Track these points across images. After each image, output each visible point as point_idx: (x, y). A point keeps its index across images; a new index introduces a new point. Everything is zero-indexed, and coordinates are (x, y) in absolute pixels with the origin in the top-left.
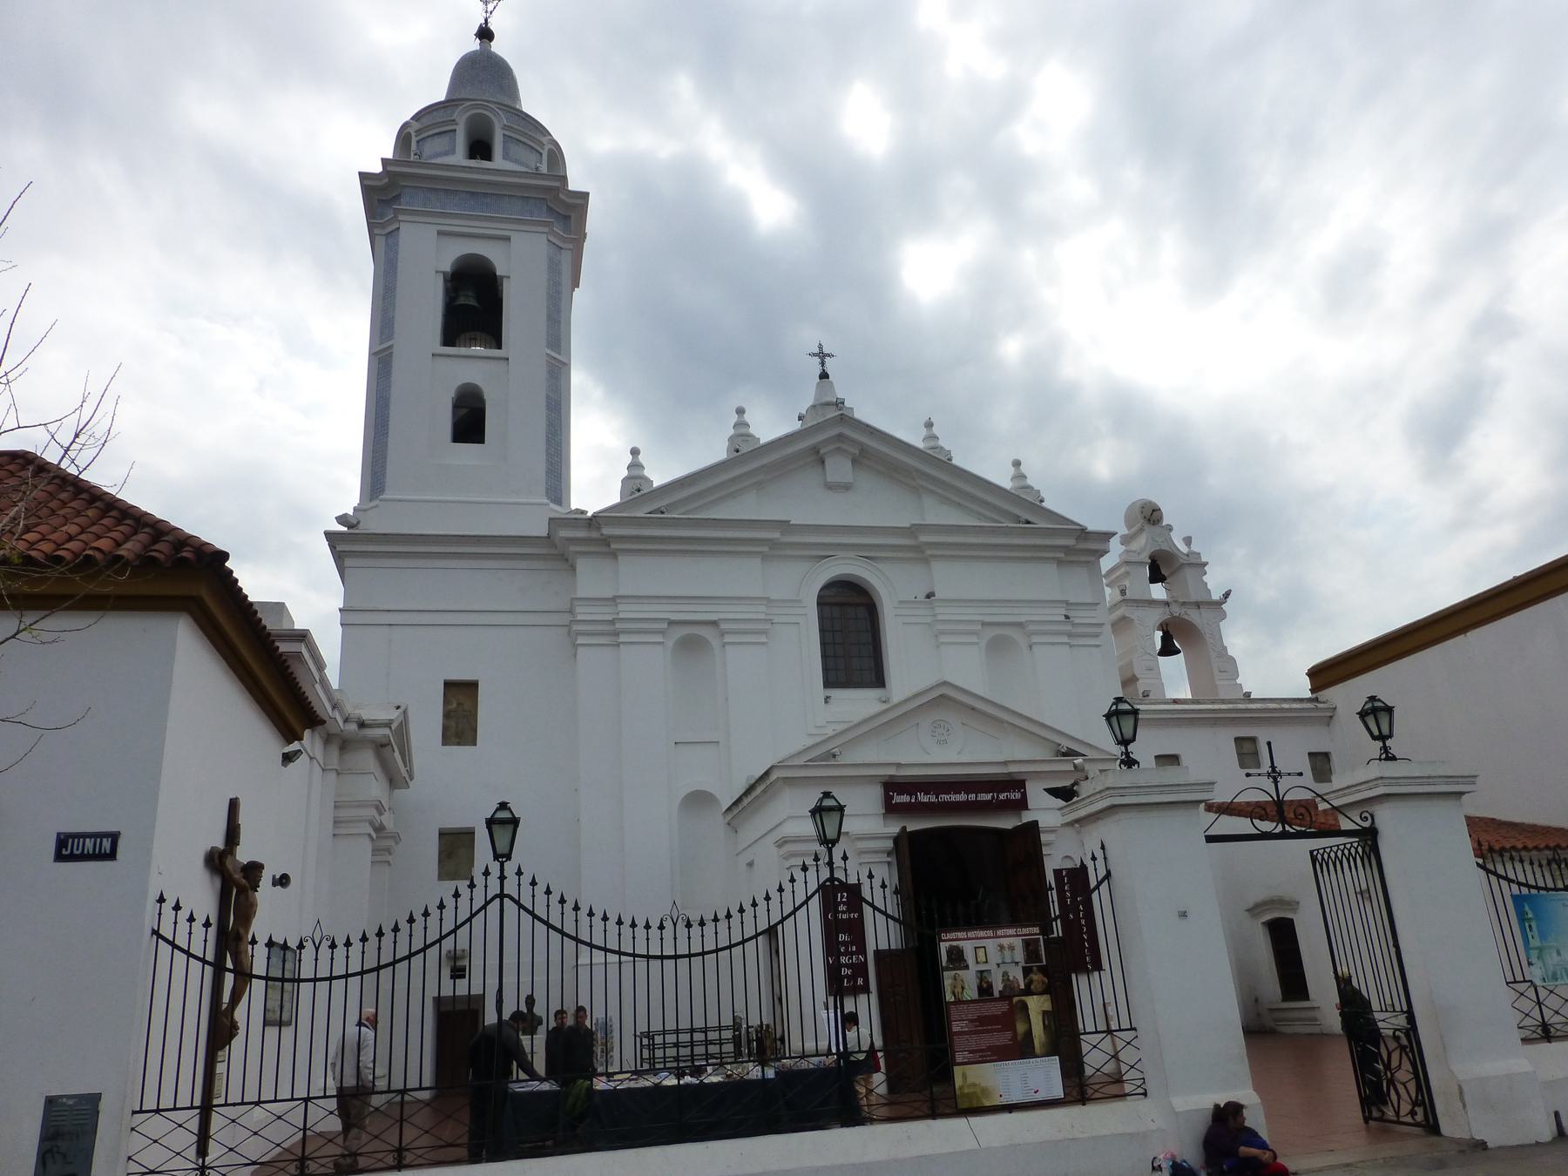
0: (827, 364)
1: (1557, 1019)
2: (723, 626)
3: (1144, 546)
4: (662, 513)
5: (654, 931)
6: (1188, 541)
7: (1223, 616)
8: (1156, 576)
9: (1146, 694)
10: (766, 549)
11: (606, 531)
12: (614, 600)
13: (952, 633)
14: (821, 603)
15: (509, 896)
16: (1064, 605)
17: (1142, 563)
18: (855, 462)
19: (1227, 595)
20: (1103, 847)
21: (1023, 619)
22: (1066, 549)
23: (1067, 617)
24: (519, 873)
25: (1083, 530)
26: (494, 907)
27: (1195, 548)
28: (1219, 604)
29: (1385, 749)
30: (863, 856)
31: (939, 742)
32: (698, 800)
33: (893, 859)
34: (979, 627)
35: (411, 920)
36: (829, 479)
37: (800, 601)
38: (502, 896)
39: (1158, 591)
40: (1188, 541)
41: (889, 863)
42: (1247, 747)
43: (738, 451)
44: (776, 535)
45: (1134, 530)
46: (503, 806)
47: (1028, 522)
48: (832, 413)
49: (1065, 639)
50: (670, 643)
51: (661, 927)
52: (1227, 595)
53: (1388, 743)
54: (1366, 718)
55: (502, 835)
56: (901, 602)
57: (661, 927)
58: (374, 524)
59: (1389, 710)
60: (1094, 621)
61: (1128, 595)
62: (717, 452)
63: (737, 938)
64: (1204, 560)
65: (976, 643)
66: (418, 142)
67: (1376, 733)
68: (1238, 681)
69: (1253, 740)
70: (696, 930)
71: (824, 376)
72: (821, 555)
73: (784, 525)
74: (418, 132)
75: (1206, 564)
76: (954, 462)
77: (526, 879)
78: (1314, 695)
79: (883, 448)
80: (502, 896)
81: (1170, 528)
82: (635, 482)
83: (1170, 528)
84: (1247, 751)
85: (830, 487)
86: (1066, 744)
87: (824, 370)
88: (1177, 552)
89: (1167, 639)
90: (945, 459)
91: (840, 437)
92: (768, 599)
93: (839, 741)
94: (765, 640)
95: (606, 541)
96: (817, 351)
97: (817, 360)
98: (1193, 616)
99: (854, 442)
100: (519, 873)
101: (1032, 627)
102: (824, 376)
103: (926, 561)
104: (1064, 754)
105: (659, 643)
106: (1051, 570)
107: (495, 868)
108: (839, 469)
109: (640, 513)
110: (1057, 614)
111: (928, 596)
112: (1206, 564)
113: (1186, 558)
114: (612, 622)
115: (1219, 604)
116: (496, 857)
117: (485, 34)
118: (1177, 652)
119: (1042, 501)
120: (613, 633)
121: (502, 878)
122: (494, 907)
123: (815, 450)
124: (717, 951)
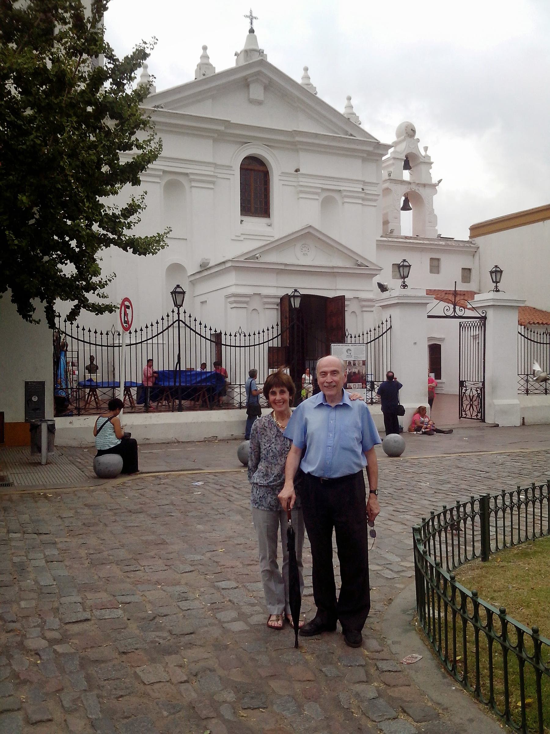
0: (254, 24)
1: (532, 388)
2: (192, 177)
3: (403, 149)
4: (162, 108)
5: (233, 337)
6: (426, 149)
7: (436, 192)
8: (407, 166)
9: (392, 232)
10: (216, 135)
15: (181, 321)
16: (362, 183)
18: (266, 88)
19: (440, 181)
20: (390, 317)
21: (341, 188)
23: (363, 189)
24: (185, 312)
25: (378, 143)
26: (176, 324)
27: (429, 153)
28: (435, 186)
29: (496, 287)
30: (266, 305)
31: (304, 254)
33: (279, 307)
34: (320, 191)
35: (147, 327)
36: (251, 97)
37: (231, 167)
38: (179, 320)
39: (406, 175)
41: (277, 309)
42: (435, 263)
43: (204, 75)
44: (222, 128)
45: (400, 139)
46: (178, 286)
47: (351, 135)
48: (256, 58)
49: (360, 202)
50: (163, 183)
51: (235, 336)
52: (440, 181)
53: (498, 284)
54: (492, 274)
55: (179, 298)
56: (282, 173)
57: (235, 336)
59: (501, 272)
60: (375, 193)
61: (392, 177)
63: (261, 342)
64: (432, 160)
65: (317, 199)
67: (494, 280)
68: (436, 228)
69: (438, 260)
70: (247, 337)
71: (252, 31)
72: (244, 142)
75: (432, 163)
76: (318, 95)
77: (187, 315)
78: (471, 240)
79: (283, 83)
80: (179, 320)
81: (418, 140)
83: (418, 140)
86: (360, 261)
87: (252, 27)
88: (420, 155)
89: (406, 201)
90: (313, 93)
91: (259, 73)
92: (215, 164)
93: (261, 251)
94: (213, 187)
96: (249, 14)
98: (422, 192)
99: (269, 77)
100: (185, 312)
101: (345, 193)
102: (252, 31)
103: (297, 151)
104: (359, 265)
105: (158, 182)
106: (358, 163)
107: (176, 309)
108: (256, 92)
110: (358, 188)
111: (297, 171)
112: (432, 163)
113: (423, 158)
115: (435, 186)
116: (176, 305)
118: (410, 209)
119: (360, 124)
121: (178, 314)
122: (176, 324)
123: (245, 79)
124: (259, 344)
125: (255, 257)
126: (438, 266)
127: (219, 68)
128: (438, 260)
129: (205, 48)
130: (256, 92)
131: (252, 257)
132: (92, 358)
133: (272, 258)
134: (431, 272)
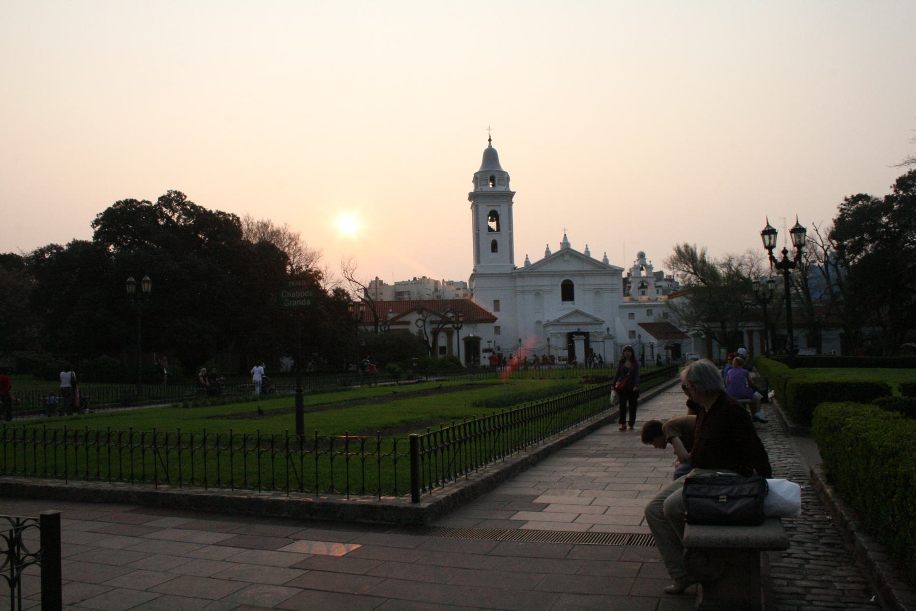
6: (650, 262)
11: (522, 274)
12: (523, 286)
21: (602, 288)
22: (613, 273)
27: (652, 263)
32: (539, 322)
40: (650, 262)
47: (605, 268)
49: (610, 292)
58: (480, 271)
62: (542, 256)
66: (480, 181)
69: (651, 310)
71: (565, 235)
73: (555, 272)
81: (646, 259)
82: (527, 262)
83: (646, 259)
84: (649, 312)
85: (565, 261)
91: (567, 252)
102: (565, 235)
108: (567, 257)
109: (527, 270)
117: (490, 140)
120: (523, 292)
125: (558, 321)
126: (651, 313)
127: (553, 252)
128: (651, 310)
129: (548, 245)
130: (567, 257)
131: (558, 321)
132: (511, 354)
134: (648, 315)
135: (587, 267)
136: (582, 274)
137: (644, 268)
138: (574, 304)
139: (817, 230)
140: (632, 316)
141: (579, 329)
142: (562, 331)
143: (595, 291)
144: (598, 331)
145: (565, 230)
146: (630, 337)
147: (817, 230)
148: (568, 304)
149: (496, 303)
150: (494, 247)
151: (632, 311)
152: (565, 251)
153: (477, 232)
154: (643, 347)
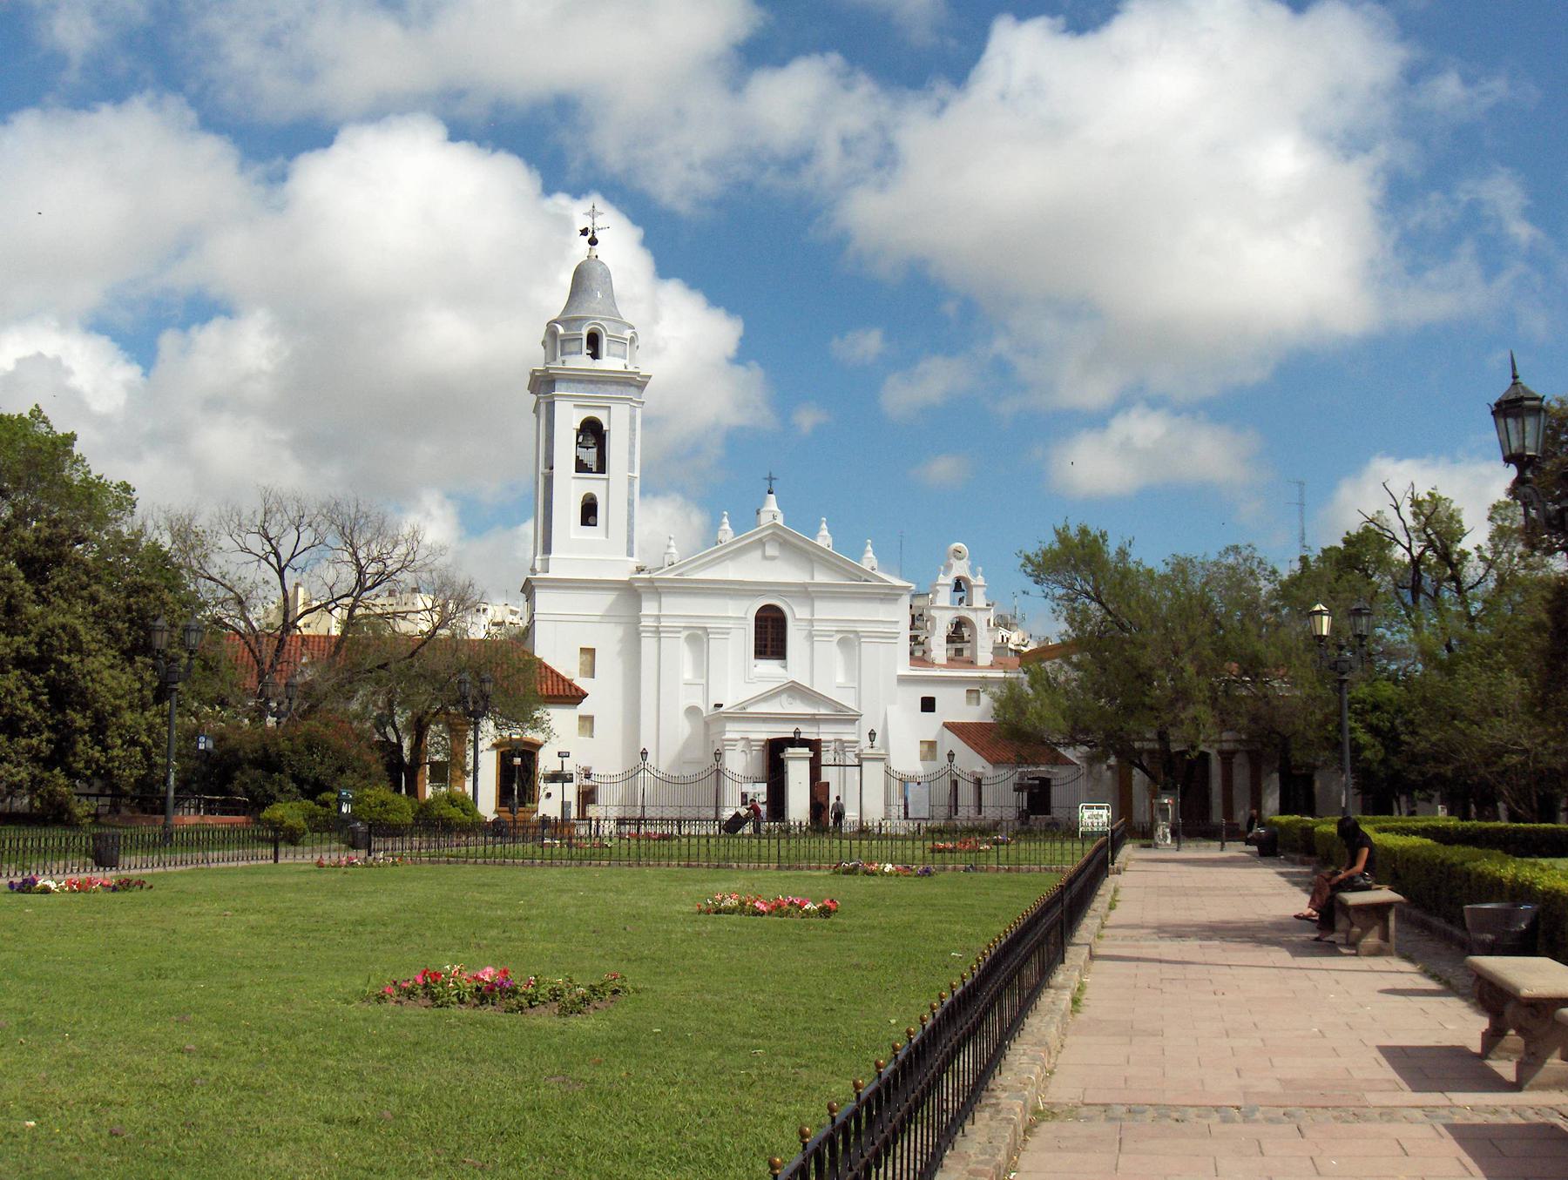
11: (656, 584)
13: (822, 636)
14: (757, 618)
17: (947, 585)
18: (780, 544)
22: (887, 594)
42: (974, 695)
74: (562, 335)
85: (765, 558)
91: (773, 533)
95: (656, 588)
97: (768, 482)
108: (771, 550)
114: (657, 627)
123: (760, 540)
131: (743, 706)
133: (764, 708)
135: (821, 577)
136: (807, 593)
137: (963, 586)
138: (785, 667)
139: (1397, 508)
140: (928, 705)
141: (797, 732)
142: (752, 736)
143: (839, 636)
144: (845, 738)
145: (771, 479)
146: (923, 759)
147: (1397, 508)
148: (770, 666)
149: (589, 652)
150: (589, 511)
151: (928, 692)
152: (770, 531)
153: (548, 470)
154: (955, 784)
